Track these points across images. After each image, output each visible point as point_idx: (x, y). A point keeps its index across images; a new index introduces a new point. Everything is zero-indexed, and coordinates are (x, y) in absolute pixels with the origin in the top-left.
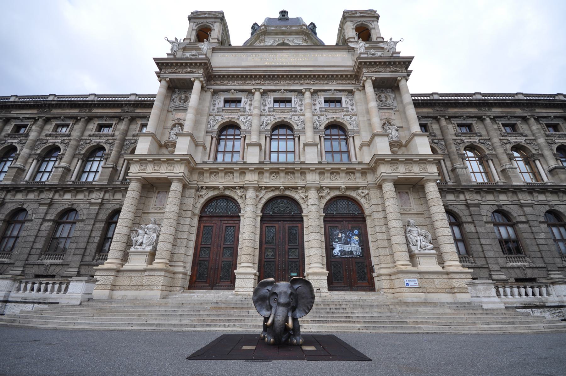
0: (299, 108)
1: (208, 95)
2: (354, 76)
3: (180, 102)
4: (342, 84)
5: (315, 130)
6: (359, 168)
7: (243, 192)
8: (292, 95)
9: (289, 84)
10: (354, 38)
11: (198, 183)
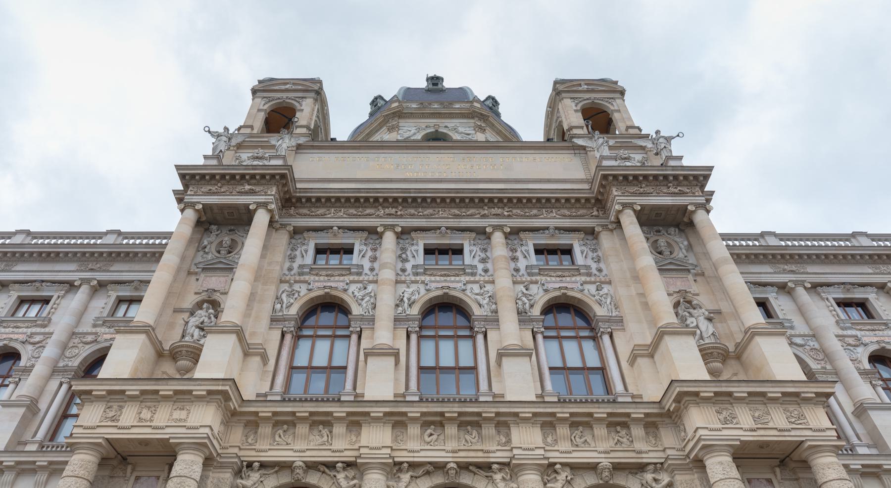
0: (480, 267)
1: (282, 239)
2: (593, 201)
3: (219, 252)
4: (570, 217)
5: (523, 317)
6: (638, 412)
7: (354, 478)
8: (463, 239)
10: (582, 127)
11: (241, 453)
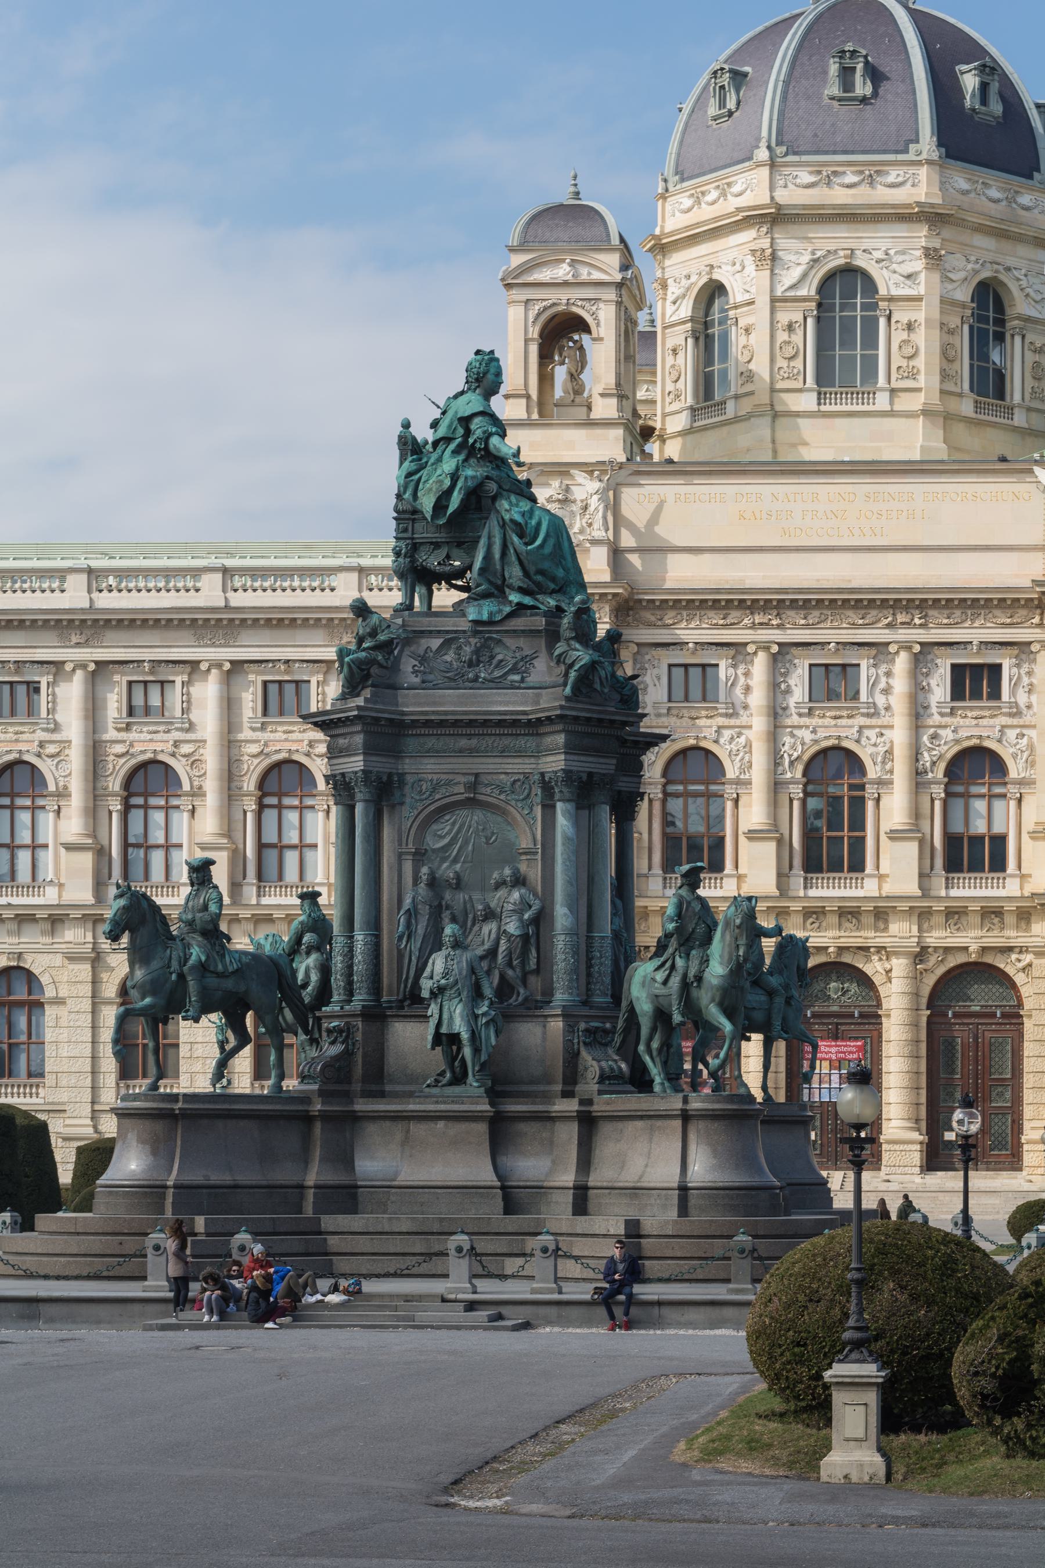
9: (854, 626)
